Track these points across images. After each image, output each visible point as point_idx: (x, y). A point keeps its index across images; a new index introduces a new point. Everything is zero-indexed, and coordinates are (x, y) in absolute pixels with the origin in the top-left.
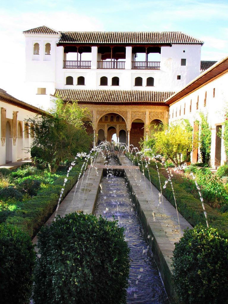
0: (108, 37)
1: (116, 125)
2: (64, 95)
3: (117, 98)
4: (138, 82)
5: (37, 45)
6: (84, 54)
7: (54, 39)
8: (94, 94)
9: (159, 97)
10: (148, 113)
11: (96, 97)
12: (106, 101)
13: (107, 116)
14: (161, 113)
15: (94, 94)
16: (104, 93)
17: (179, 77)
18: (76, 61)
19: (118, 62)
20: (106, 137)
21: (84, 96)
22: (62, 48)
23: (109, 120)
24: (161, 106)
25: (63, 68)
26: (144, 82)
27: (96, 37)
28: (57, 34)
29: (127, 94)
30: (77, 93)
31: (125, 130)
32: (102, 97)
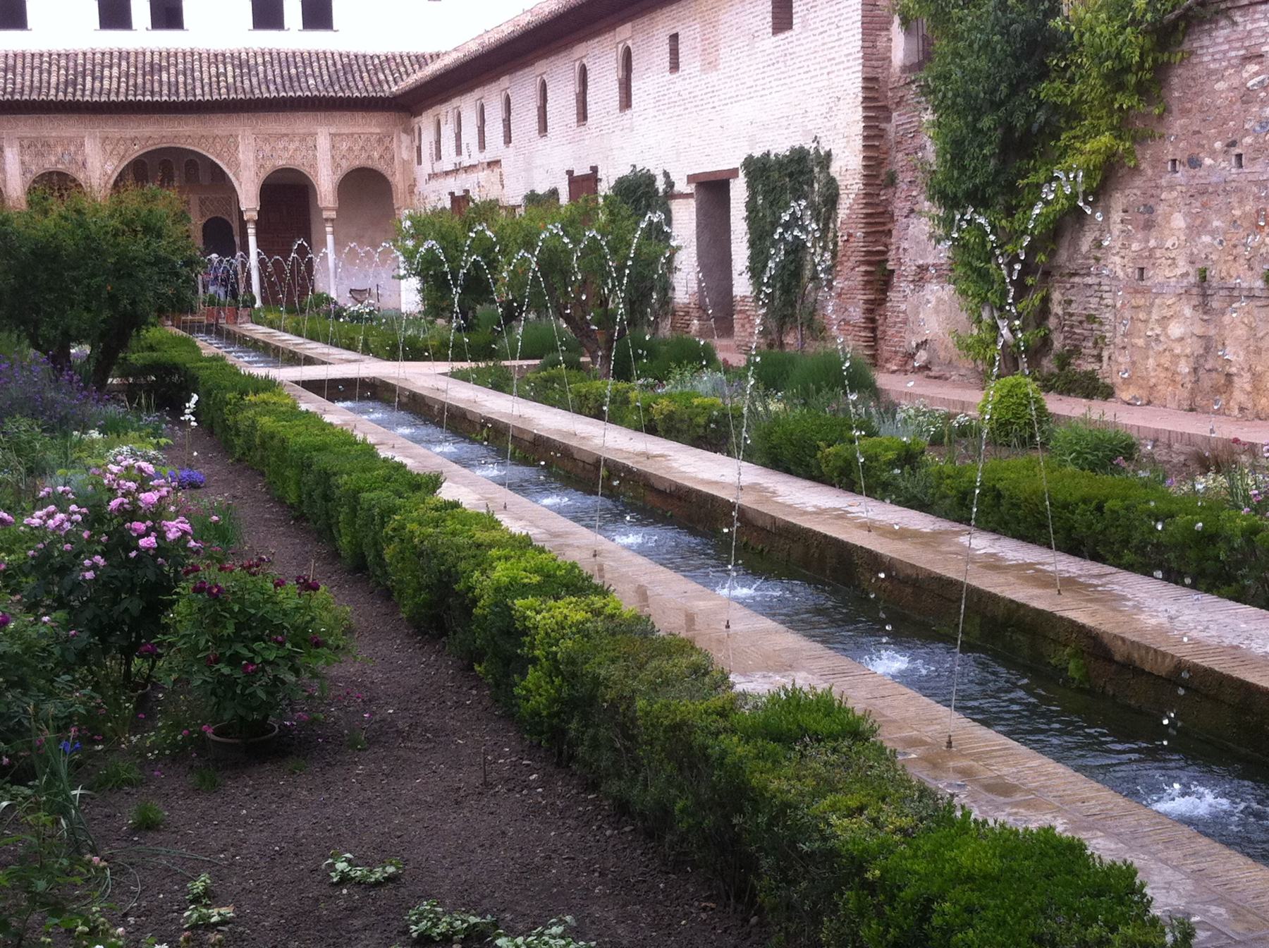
8: (80, 69)
9: (365, 75)
10: (323, 142)
11: (89, 79)
12: (139, 98)
13: (144, 163)
14: (380, 141)
15: (80, 69)
16: (124, 64)
21: (36, 79)
29: (225, 64)
31: (226, 217)
32: (119, 78)
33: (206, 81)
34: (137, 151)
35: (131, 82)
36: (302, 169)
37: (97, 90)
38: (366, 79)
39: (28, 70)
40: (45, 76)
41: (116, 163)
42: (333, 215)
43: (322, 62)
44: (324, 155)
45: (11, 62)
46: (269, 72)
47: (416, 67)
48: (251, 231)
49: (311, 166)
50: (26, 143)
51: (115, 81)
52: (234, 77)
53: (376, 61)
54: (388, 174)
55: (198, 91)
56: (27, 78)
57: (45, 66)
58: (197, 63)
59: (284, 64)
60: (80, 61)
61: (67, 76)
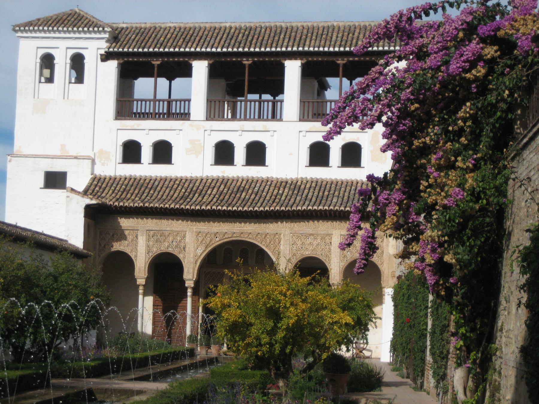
0: (240, 36)
2: (111, 191)
3: (253, 200)
5: (48, 61)
6: (178, 82)
7: (93, 47)
8: (194, 189)
11: (197, 195)
15: (194, 189)
16: (222, 186)
18: (150, 101)
19: (264, 101)
22: (113, 65)
25: (116, 119)
27: (207, 36)
28: (101, 29)
30: (150, 186)
33: (268, 198)
34: (217, 242)
35: (221, 198)
36: (321, 258)
37: (197, 202)
40: (172, 192)
41: (203, 249)
43: (348, 188)
45: (156, 183)
46: (310, 194)
49: (328, 256)
50: (152, 233)
51: (212, 196)
52: (286, 197)
55: (259, 204)
56: (161, 193)
57: (176, 186)
59: (322, 189)
60: (197, 184)
61: (185, 193)
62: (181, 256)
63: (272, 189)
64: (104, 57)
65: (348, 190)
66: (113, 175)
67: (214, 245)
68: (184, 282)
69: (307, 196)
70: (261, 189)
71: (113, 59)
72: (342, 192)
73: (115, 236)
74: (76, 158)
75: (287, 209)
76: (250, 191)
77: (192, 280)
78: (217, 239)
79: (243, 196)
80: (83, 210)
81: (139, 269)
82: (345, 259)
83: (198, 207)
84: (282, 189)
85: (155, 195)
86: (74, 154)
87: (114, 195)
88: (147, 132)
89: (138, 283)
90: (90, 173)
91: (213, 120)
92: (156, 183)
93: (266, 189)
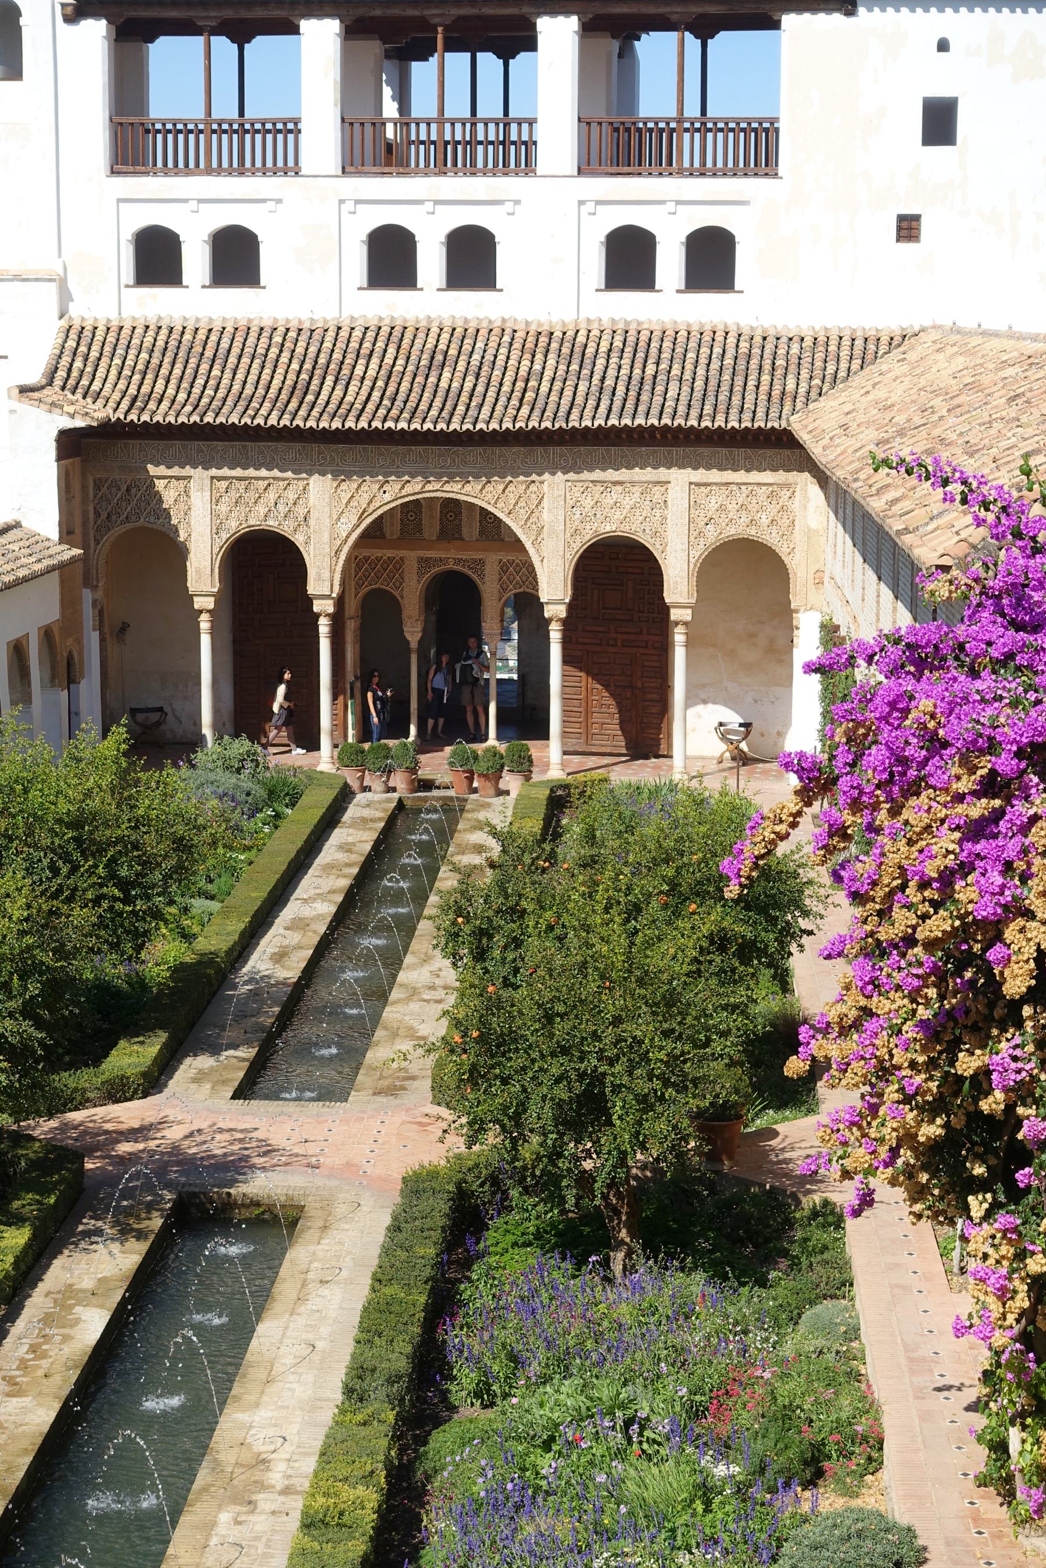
1: (481, 562)
2: (114, 372)
4: (629, 258)
8: (322, 360)
9: (766, 378)
12: (390, 424)
15: (322, 360)
16: (391, 351)
17: (908, 228)
20: (414, 645)
21: (252, 378)
23: (431, 528)
24: (769, 452)
25: (113, 172)
26: (670, 262)
30: (209, 353)
33: (506, 388)
35: (391, 389)
38: (764, 388)
39: (245, 360)
42: (686, 615)
43: (705, 351)
44: (676, 516)
46: (611, 373)
47: (856, 364)
48: (555, 635)
51: (368, 383)
53: (795, 349)
54: (783, 551)
56: (240, 376)
58: (503, 351)
59: (641, 355)
61: (299, 373)
62: (299, 539)
63: (515, 355)
64: (69, 10)
65: (703, 360)
66: (113, 316)
67: (380, 512)
68: (309, 601)
69: (603, 380)
70: (489, 357)
71: (95, 15)
72: (689, 366)
73: (133, 491)
74: (17, 278)
75: (557, 426)
76: (461, 366)
77: (328, 597)
78: (387, 497)
79: (444, 384)
80: (54, 445)
81: (198, 571)
82: (702, 543)
83: (336, 424)
84: (539, 357)
85: (225, 381)
86: (14, 268)
87: (122, 386)
88: (193, 207)
89: (196, 606)
90: (56, 315)
91: (360, 173)
92: (225, 344)
93: (501, 358)
